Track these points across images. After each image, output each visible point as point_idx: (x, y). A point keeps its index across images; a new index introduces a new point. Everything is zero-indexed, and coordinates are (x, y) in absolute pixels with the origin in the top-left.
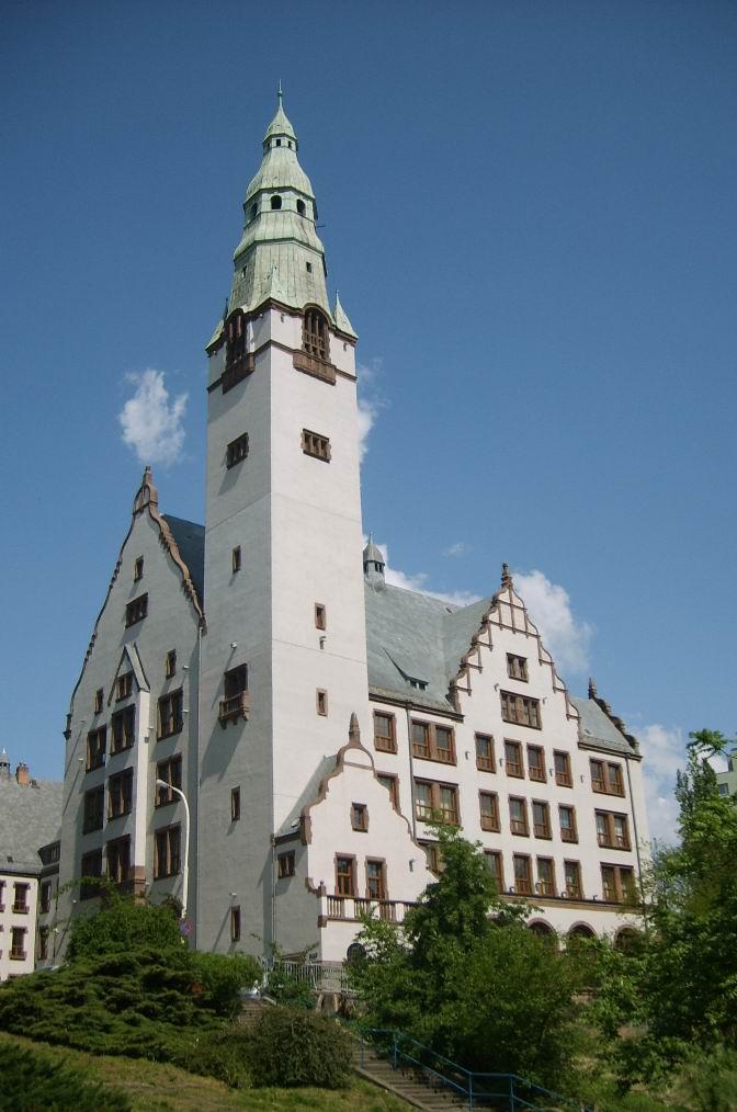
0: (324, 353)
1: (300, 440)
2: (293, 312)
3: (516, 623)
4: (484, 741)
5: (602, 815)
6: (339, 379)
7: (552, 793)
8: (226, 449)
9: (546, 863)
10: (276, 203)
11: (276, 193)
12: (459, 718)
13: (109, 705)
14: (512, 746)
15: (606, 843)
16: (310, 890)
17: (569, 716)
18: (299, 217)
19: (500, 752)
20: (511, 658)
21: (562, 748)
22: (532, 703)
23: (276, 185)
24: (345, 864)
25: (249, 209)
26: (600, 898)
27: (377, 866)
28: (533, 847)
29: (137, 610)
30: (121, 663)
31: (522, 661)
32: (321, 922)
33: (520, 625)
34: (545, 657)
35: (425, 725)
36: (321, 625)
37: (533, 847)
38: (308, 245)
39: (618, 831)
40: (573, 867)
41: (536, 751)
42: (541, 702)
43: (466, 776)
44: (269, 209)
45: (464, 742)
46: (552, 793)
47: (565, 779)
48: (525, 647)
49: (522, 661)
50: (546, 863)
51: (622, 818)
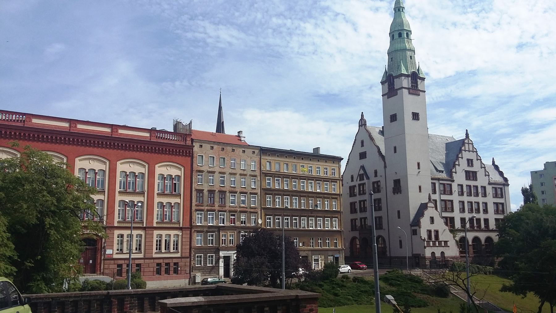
0: (417, 86)
1: (411, 116)
3: (470, 149)
5: (496, 204)
6: (421, 93)
7: (480, 199)
9: (478, 220)
12: (453, 181)
13: (357, 181)
14: (469, 187)
16: (422, 239)
17: (486, 175)
20: (468, 160)
23: (400, 29)
25: (391, 35)
26: (495, 229)
29: (363, 156)
30: (360, 170)
31: (472, 160)
32: (425, 247)
33: (471, 149)
35: (444, 184)
36: (419, 168)
38: (410, 50)
39: (501, 208)
40: (486, 221)
41: (476, 187)
43: (455, 198)
46: (480, 199)
47: (485, 195)
49: (472, 160)
50: (478, 220)
51: (502, 204)
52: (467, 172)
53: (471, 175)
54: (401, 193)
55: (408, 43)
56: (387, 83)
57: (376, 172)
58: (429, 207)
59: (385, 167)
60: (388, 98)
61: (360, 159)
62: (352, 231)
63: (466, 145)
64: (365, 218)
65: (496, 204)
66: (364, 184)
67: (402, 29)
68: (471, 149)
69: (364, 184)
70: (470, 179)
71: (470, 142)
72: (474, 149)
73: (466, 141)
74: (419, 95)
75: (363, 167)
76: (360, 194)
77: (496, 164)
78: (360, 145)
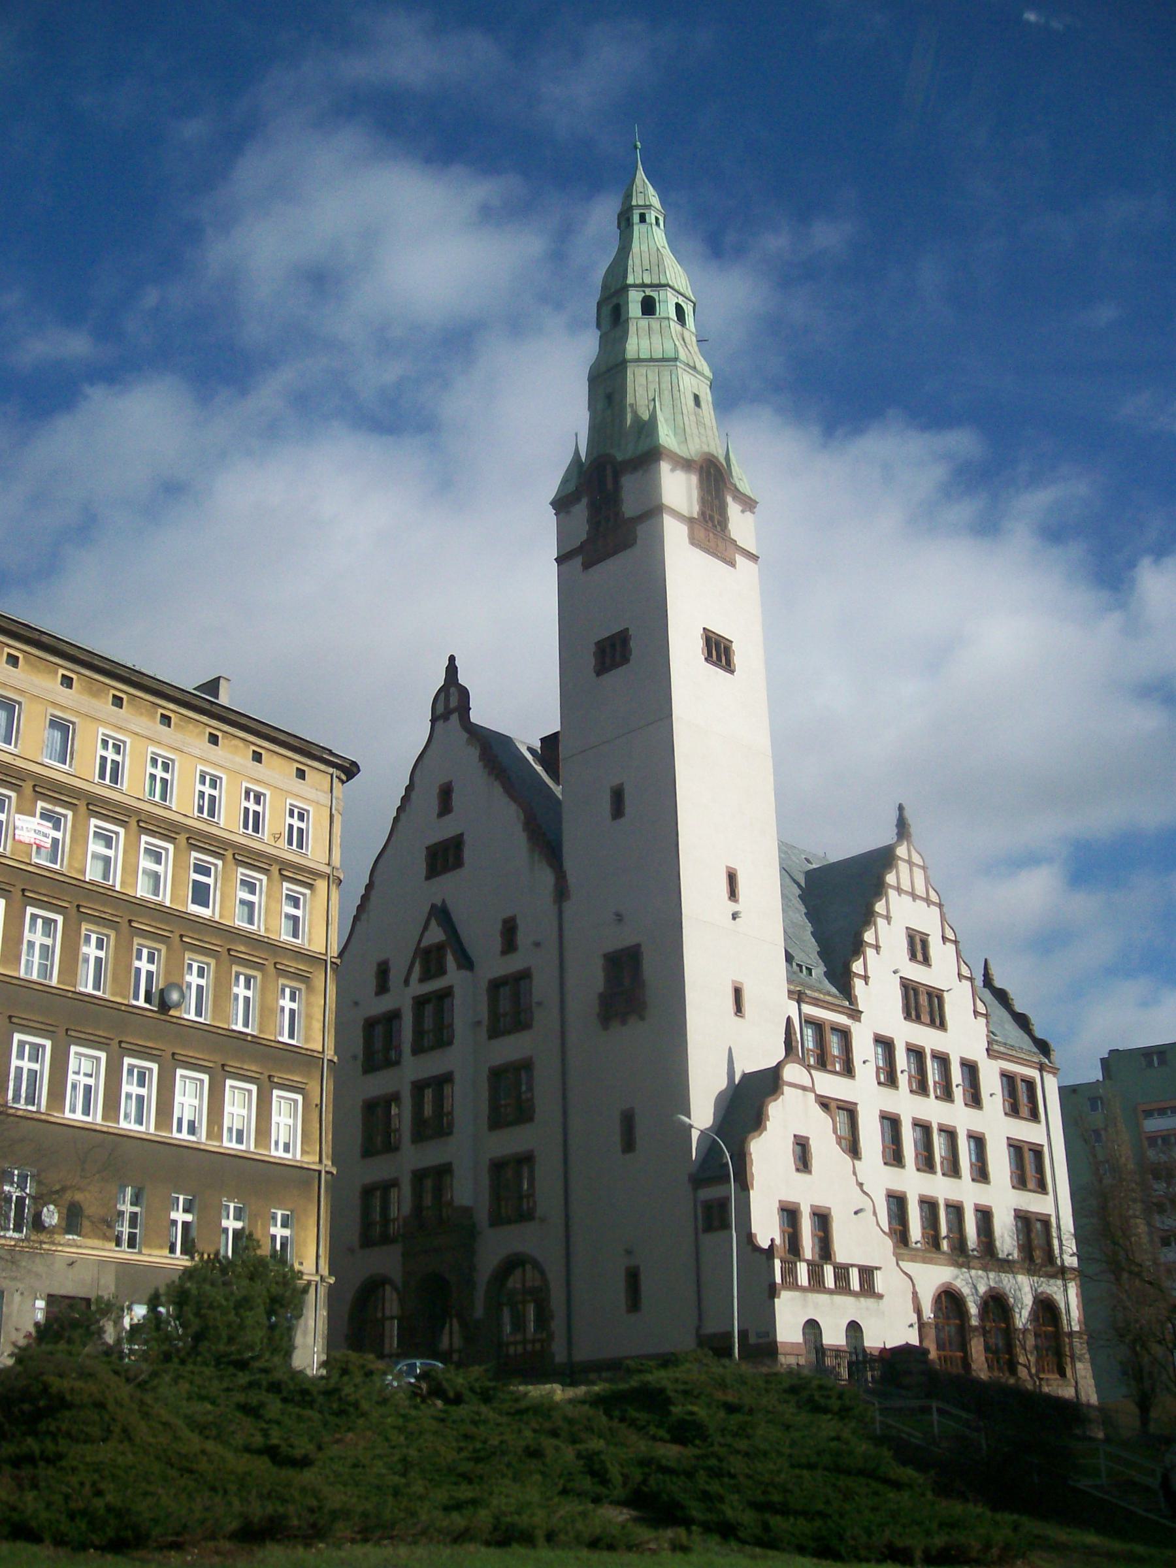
2: (686, 464)
4: (885, 1044)
7: (958, 1115)
8: (593, 649)
10: (649, 307)
11: (649, 292)
13: (407, 982)
15: (1020, 1181)
17: (976, 1013)
18: (679, 327)
19: (902, 1060)
21: (970, 1056)
22: (936, 997)
23: (647, 281)
24: (790, 1214)
27: (822, 1219)
28: (941, 1188)
30: (426, 927)
34: (950, 935)
37: (941, 1188)
40: (985, 1216)
42: (945, 994)
44: (640, 314)
45: (864, 1050)
46: (958, 1115)
48: (928, 921)
50: (956, 1210)
52: (909, 989)
53: (923, 1000)
54: (642, 1018)
55: (683, 343)
56: (584, 501)
57: (509, 929)
58: (570, 1354)
59: (561, 892)
60: (587, 566)
61: (428, 878)
62: (362, 1247)
63: (903, 867)
64: (443, 1171)
65: (1017, 1148)
66: (446, 994)
67: (656, 282)
68: (920, 890)
69: (446, 994)
70: (918, 1019)
71: (916, 859)
72: (932, 893)
73: (901, 851)
74: (732, 564)
75: (441, 914)
76: (417, 1050)
77: (998, 983)
78: (434, 804)
